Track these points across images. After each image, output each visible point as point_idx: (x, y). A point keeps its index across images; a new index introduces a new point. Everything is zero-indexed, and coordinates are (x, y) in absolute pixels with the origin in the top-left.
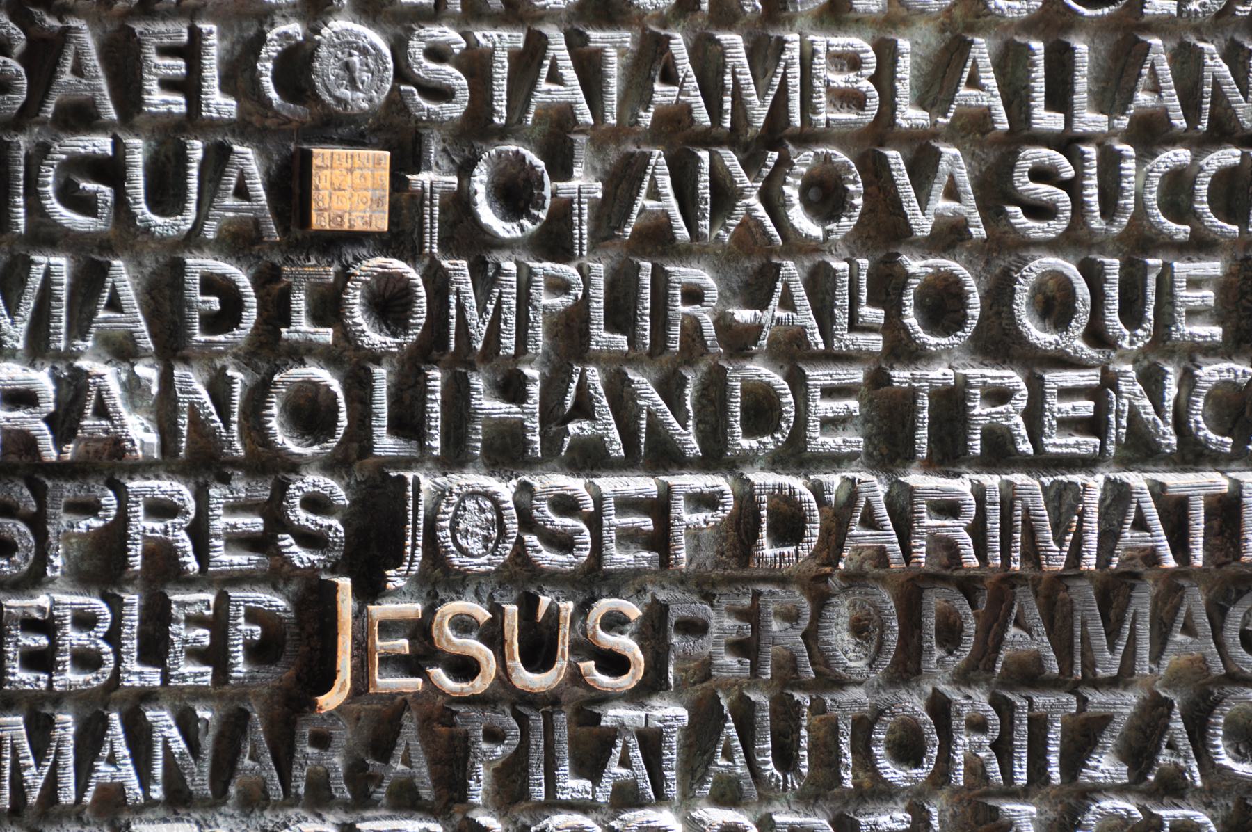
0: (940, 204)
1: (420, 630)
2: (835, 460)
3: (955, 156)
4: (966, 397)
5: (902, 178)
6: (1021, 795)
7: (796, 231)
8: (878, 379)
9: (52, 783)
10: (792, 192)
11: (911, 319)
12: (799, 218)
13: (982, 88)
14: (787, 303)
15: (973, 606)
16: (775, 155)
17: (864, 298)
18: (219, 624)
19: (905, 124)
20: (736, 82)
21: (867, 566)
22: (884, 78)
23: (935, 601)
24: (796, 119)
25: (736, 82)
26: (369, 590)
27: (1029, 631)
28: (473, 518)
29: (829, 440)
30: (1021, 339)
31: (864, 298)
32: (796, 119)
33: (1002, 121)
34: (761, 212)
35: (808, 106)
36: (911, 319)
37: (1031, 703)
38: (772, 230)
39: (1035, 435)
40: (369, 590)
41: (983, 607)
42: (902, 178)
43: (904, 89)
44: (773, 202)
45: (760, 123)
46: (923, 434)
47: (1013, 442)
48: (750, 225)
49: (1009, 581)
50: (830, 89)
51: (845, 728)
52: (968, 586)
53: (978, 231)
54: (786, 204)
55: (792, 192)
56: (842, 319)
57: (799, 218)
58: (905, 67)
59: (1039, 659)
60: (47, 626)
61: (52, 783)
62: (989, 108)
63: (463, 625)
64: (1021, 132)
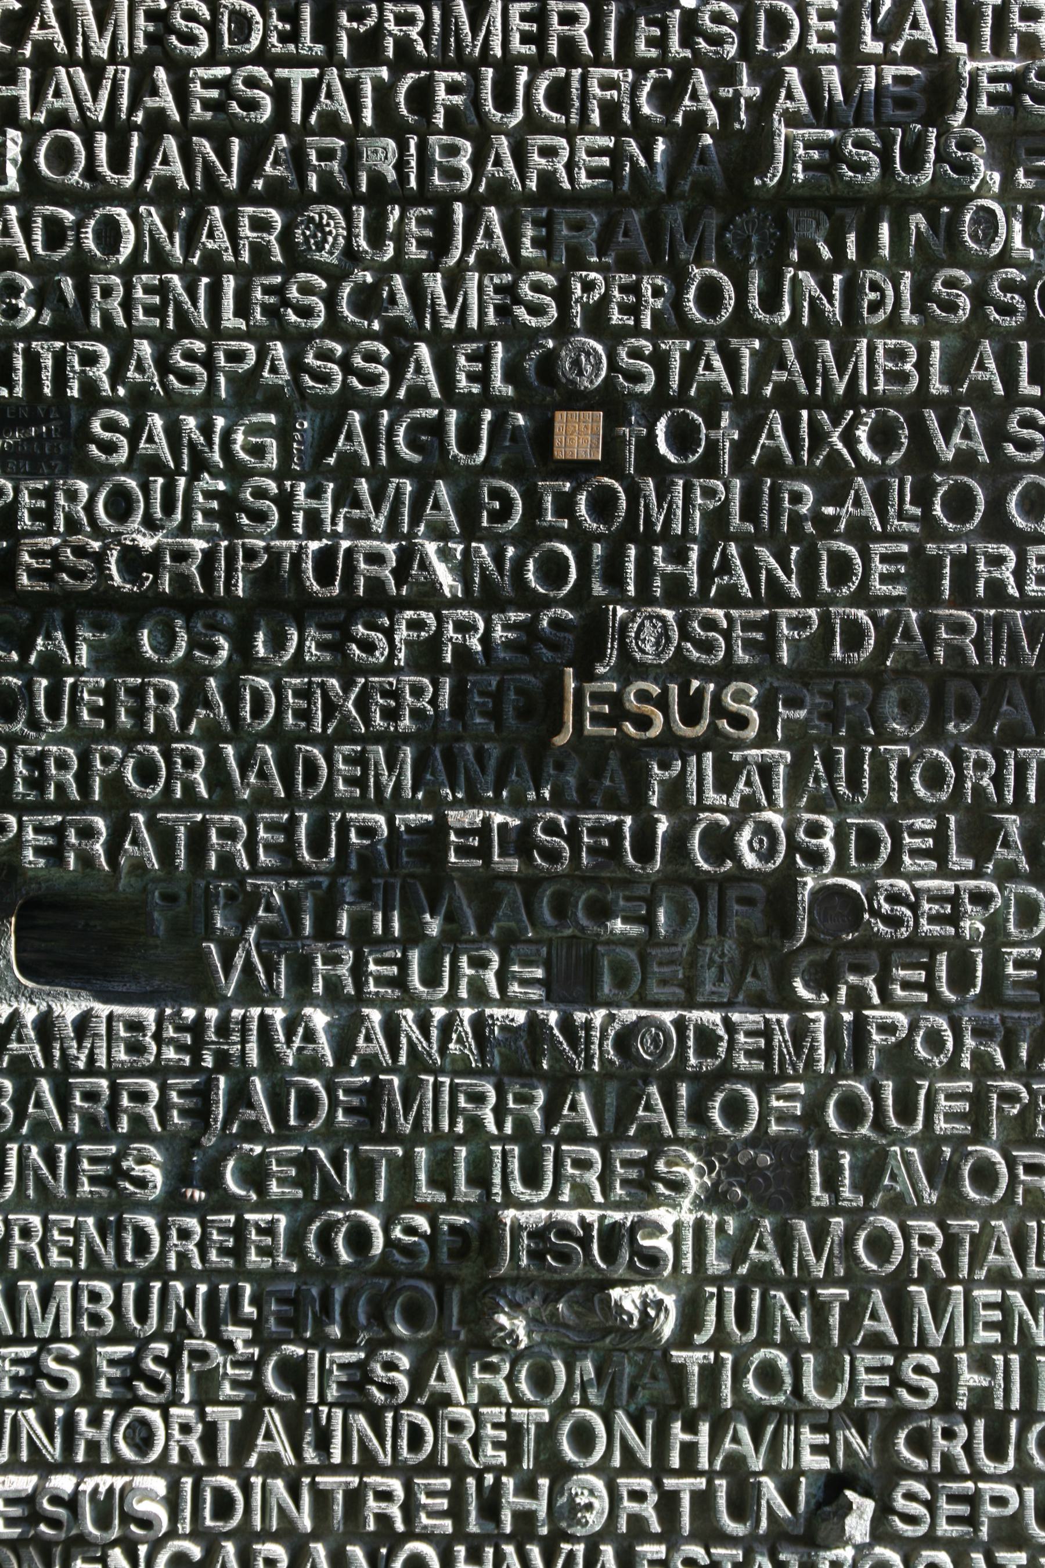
0: (957, 439)
1: (616, 700)
2: (888, 601)
3: (968, 412)
4: (976, 561)
5: (934, 424)
6: (1008, 810)
7: (864, 459)
8: (918, 551)
9: (398, 787)
10: (862, 433)
11: (938, 511)
12: (865, 449)
13: (985, 369)
14: (858, 503)
15: (980, 692)
16: (851, 412)
17: (908, 499)
18: (498, 696)
19: (934, 392)
20: (824, 367)
21: (909, 666)
22: (923, 365)
23: (953, 687)
24: (864, 391)
25: (824, 367)
26: (585, 675)
27: (1016, 708)
28: (649, 635)
29: (884, 588)
30: (1012, 526)
31: (908, 499)
32: (864, 391)
33: (999, 389)
34: (840, 446)
35: (872, 382)
36: (938, 511)
37: (1016, 752)
38: (848, 457)
39: (1020, 584)
40: (585, 675)
41: (986, 692)
42: (934, 424)
43: (935, 369)
44: (850, 440)
45: (841, 391)
46: (946, 582)
47: (1006, 586)
48: (835, 453)
49: (1002, 679)
50: (886, 372)
51: (894, 766)
52: (977, 679)
53: (984, 458)
54: (858, 441)
55: (862, 433)
56: (892, 511)
57: (865, 449)
58: (936, 357)
59: (1023, 726)
60: (394, 694)
61: (398, 787)
62: (990, 381)
63: (643, 696)
64: (1013, 398)
